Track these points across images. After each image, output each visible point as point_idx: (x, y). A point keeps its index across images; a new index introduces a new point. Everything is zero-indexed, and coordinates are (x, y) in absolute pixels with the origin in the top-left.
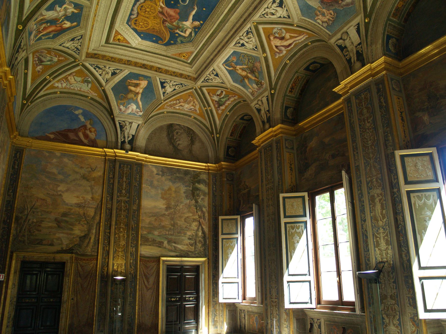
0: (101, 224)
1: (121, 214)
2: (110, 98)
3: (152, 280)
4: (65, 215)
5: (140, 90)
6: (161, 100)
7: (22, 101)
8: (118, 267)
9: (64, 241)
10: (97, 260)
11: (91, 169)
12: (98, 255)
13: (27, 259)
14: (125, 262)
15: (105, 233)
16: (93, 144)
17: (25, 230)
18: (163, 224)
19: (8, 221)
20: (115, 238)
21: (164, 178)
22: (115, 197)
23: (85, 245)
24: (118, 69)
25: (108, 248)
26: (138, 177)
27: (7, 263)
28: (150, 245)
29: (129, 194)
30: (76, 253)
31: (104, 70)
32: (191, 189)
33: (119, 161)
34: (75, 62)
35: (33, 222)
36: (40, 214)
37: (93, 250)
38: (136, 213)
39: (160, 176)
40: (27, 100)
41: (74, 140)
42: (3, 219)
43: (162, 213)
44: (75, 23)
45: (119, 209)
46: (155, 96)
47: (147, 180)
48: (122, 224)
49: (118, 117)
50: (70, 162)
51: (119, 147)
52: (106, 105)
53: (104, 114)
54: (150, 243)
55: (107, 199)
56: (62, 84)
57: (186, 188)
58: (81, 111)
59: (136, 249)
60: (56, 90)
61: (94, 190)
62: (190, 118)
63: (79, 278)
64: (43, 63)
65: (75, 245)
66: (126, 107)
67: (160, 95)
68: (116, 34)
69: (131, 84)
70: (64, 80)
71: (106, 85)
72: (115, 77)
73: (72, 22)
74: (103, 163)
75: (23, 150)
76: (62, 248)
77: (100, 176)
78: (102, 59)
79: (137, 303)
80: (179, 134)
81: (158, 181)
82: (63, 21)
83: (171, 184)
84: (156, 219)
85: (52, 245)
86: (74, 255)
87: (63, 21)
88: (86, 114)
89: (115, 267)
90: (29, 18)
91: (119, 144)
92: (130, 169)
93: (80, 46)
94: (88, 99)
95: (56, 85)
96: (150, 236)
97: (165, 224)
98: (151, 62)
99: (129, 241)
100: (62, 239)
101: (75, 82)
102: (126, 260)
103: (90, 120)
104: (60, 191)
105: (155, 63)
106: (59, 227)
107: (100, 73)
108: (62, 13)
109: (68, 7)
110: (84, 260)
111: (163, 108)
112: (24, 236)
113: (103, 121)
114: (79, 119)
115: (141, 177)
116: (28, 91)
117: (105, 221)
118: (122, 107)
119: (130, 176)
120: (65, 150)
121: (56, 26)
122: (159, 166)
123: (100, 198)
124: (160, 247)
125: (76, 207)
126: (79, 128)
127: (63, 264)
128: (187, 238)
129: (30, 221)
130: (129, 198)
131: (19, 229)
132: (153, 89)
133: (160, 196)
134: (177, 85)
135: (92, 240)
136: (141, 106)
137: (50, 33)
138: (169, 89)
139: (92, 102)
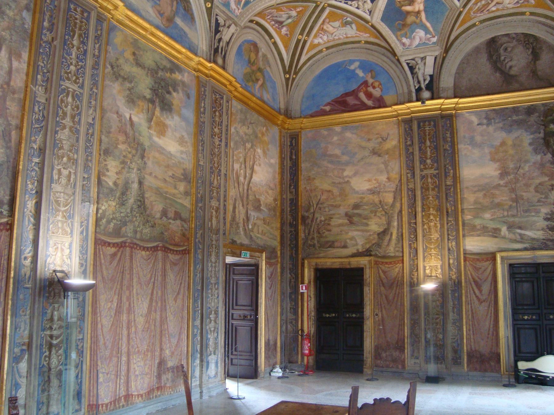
0: (403, 212)
1: (429, 195)
2: (384, 34)
3: (486, 288)
4: (356, 206)
6: (458, 9)
8: (431, 270)
9: (358, 241)
10: (403, 263)
11: (382, 138)
12: (403, 256)
13: (320, 267)
14: (441, 262)
15: (410, 223)
16: (380, 103)
17: (313, 231)
18: (497, 201)
19: (294, 223)
20: (423, 230)
21: (491, 129)
22: (418, 172)
23: (386, 244)
25: (415, 246)
26: (448, 135)
27: (300, 271)
28: (479, 236)
29: (438, 163)
30: (376, 256)
32: (542, 135)
34: (317, 6)
35: (321, 221)
36: (327, 210)
37: (397, 249)
38: (452, 190)
39: (485, 127)
40: (290, 74)
41: (355, 105)
42: (288, 222)
43: (495, 184)
45: (425, 188)
46: (445, 6)
47: (464, 137)
48: (431, 209)
50: (354, 136)
51: (414, 98)
52: (383, 44)
53: (388, 58)
54: (478, 233)
55: (407, 177)
56: (321, 37)
57: (532, 136)
58: (357, 64)
59: (456, 243)
60: (320, 48)
61: (389, 167)
62: (524, 17)
63: (382, 288)
64: (284, 24)
65: (373, 245)
66: (410, 38)
70: (320, 32)
74: (396, 126)
75: (298, 135)
76: (358, 250)
77: (395, 147)
79: (464, 321)
80: (509, 49)
81: (482, 135)
83: (504, 134)
84: (485, 194)
85: (345, 247)
86: (372, 257)
88: (364, 66)
89: (428, 272)
91: (414, 95)
92: (435, 126)
94: (362, 45)
95: (316, 41)
96: (477, 222)
97: (502, 200)
99: (444, 233)
100: (357, 238)
101: (335, 30)
102: (442, 260)
103: (371, 71)
104: (346, 177)
106: (351, 223)
107: (356, 6)
110: (386, 263)
111: (468, 17)
112: (313, 238)
113: (386, 67)
114: (357, 75)
115: (452, 134)
116: (287, 63)
117: (409, 207)
119: (436, 137)
120: (346, 121)
122: (481, 111)
123: (397, 176)
124: (496, 237)
125: (369, 194)
126: (359, 87)
127: (360, 271)
128: (541, 218)
129: (318, 220)
130: (437, 169)
131: (307, 232)
133: (489, 157)
135: (394, 237)
136: (431, 29)
139: (368, 46)
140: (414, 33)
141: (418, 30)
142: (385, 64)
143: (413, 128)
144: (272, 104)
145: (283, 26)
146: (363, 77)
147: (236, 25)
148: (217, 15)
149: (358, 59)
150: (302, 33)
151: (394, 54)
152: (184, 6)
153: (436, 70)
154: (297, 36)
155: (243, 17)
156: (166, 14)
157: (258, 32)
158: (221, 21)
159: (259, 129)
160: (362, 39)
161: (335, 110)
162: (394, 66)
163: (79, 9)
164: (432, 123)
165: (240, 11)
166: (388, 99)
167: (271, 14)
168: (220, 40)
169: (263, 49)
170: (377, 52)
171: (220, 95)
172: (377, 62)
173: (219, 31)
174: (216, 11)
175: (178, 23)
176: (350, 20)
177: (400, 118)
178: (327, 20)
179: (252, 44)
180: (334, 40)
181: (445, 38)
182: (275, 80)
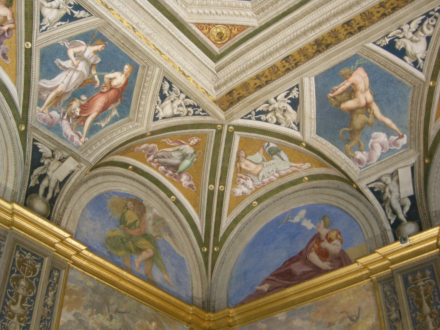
2: (327, 154)
5: (365, 96)
6: (424, 82)
7: (201, 251)
24: (291, 90)
31: (274, 110)
33: (401, 271)
34: (219, 133)
40: (206, 244)
41: (304, 273)
46: (404, 84)
49: (363, 179)
50: (306, 322)
52: (333, 172)
53: (344, 191)
56: (243, 184)
58: (303, 213)
60: (247, 202)
66: (367, 149)
67: (412, 74)
68: (206, 31)
69: (339, 98)
70: (240, 175)
71: (303, 135)
72: (303, 106)
73: (121, 70)
74: (370, 293)
78: (250, 93)
82: (101, 78)
87: (101, 78)
88: (313, 213)
90: (26, 107)
91: (390, 234)
93: (187, 97)
95: (239, 191)
98: (320, 24)
101: (260, 168)
103: (323, 218)
105: (327, 20)
107: (275, 120)
108: (82, 66)
109: (77, 50)
113: (343, 205)
114: (305, 228)
116: (201, 230)
118: (359, 155)
121: (102, 93)
132: (386, 73)
134: (421, 25)
136: (394, 126)
137: (105, 108)
138: (418, 49)
139: (315, 183)
140: (371, 141)
141: (375, 134)
142: (341, 202)
143: (397, 290)
144: (174, 289)
145: (180, 173)
146: (313, 228)
147: (77, 158)
148: (34, 140)
149: (302, 205)
150: (212, 181)
151: (350, 182)
153: (417, 186)
154: (206, 187)
155: (90, 148)
157: (144, 185)
159: (139, 322)
160: (304, 174)
161: (277, 288)
162: (354, 201)
164: (428, 272)
165: (83, 140)
166: (350, 252)
167: (151, 151)
168: (42, 177)
169: (155, 207)
170: (328, 188)
172: (328, 202)
173: (43, 164)
174: (32, 135)
176: (275, 145)
177: (374, 277)
178: (243, 154)
179: (131, 200)
180: (264, 185)
181: (419, 135)
182: (182, 255)
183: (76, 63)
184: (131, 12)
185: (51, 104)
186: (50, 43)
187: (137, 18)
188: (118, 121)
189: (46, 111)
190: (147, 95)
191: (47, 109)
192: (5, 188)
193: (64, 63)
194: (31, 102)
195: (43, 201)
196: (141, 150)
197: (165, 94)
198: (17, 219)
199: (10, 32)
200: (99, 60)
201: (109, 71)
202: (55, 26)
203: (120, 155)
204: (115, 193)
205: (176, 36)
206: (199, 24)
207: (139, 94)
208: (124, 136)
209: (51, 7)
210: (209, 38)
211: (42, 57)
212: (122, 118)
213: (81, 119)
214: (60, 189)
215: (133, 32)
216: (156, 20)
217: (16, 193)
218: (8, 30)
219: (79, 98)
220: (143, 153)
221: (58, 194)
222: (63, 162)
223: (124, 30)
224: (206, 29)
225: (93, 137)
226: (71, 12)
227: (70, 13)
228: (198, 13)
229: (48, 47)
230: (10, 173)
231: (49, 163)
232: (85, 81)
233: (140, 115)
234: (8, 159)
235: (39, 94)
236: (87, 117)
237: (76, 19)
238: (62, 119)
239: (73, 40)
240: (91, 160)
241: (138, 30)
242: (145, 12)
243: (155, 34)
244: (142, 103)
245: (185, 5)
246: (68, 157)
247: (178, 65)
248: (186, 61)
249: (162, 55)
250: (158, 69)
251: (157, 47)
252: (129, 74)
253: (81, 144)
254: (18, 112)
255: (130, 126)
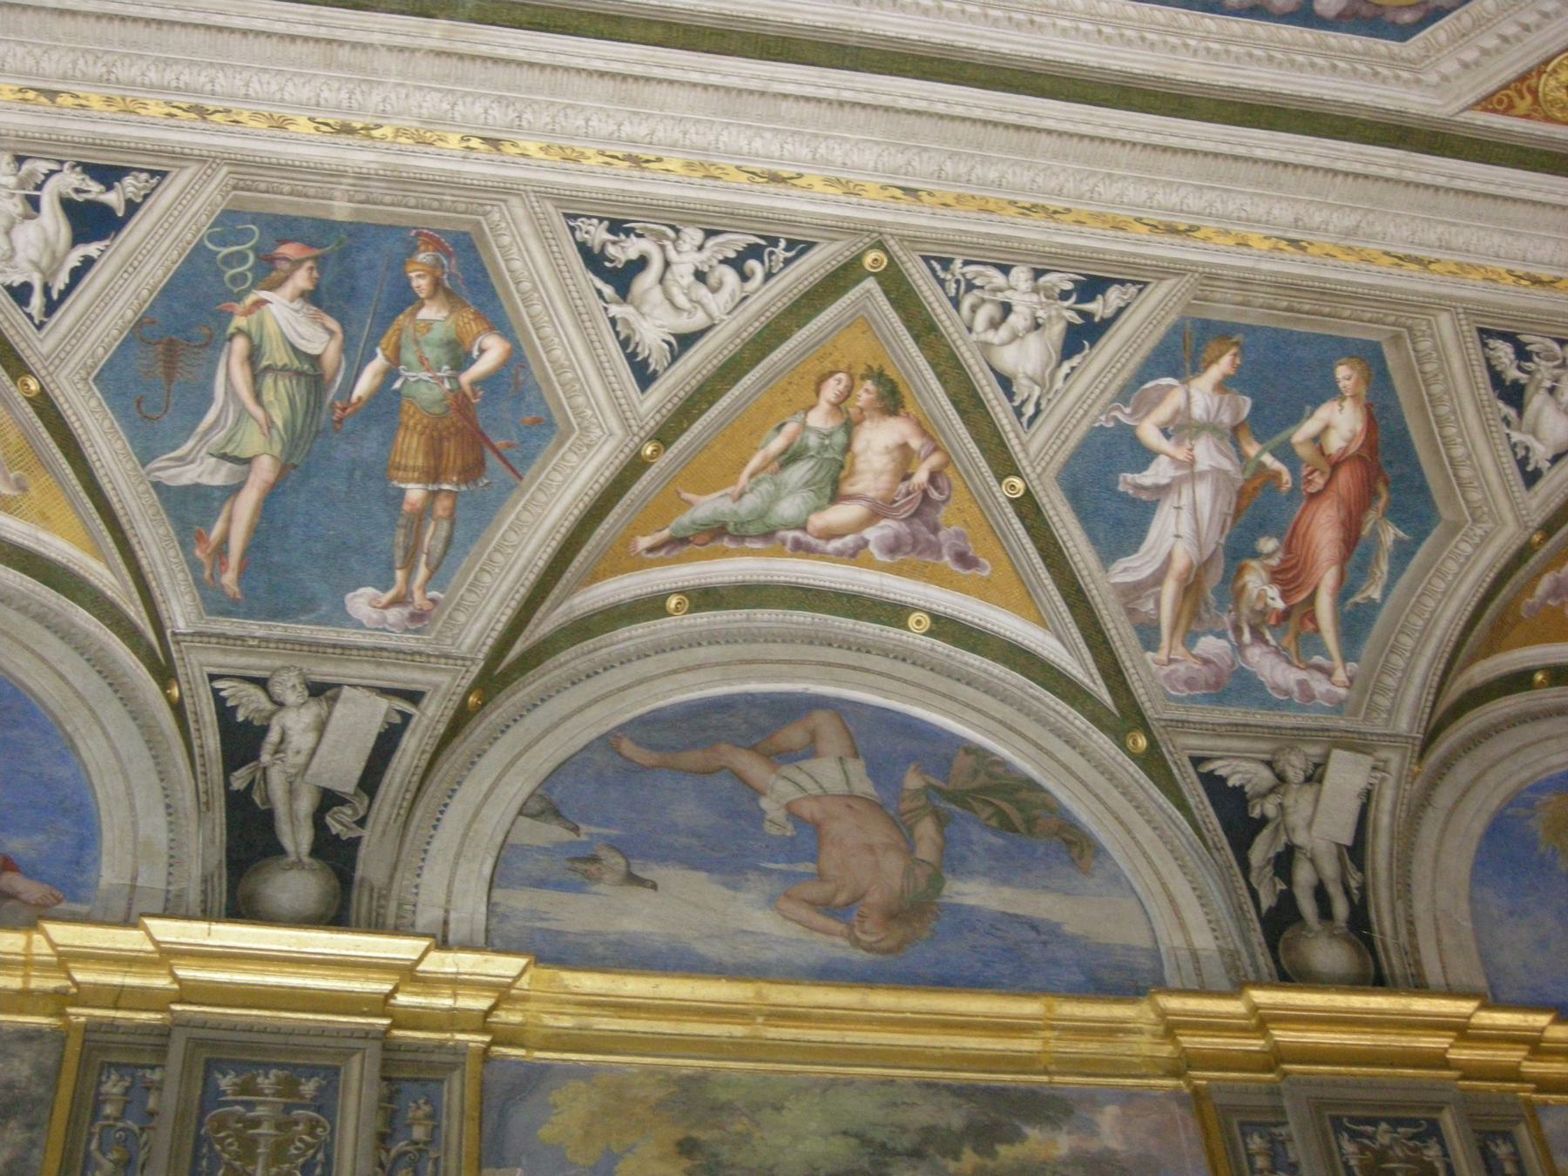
44: (1342, 372)
68: (1524, 105)
73: (1331, 391)
82: (1286, 453)
87: (1286, 453)
90: (1113, 672)
108: (1206, 453)
109: (1163, 412)
121: (1313, 497)
137: (1351, 537)
147: (1357, 744)
148: (1197, 761)
152: (1000, 813)
155: (1379, 689)
156: (874, 897)
158: (1243, 772)
163: (266, 1082)
165: (1340, 675)
168: (1284, 863)
171: (1396, 1123)
173: (1263, 821)
174: (1179, 749)
175: (970, 901)
183: (1181, 454)
184: (1256, 200)
185: (1183, 622)
186: (1072, 443)
187: (1284, 204)
188: (1413, 554)
189: (1180, 652)
190: (1457, 420)
191: (1177, 642)
192: (1194, 955)
193: (1148, 478)
194: (1122, 651)
195: (1332, 936)
196: (1543, 604)
197: (1515, 382)
198: (1284, 1036)
199: (941, 482)
200: (1246, 404)
201: (1296, 418)
202: (1059, 384)
203: (1486, 656)
204: (1537, 788)
205: (1441, 181)
206: (1488, 98)
207: (1431, 432)
208: (1464, 589)
209: (1015, 337)
210: (1548, 119)
211: (1075, 495)
212: (1418, 541)
213: (1299, 615)
214: (1361, 868)
215: (1299, 256)
216: (1347, 174)
217: (1234, 955)
218: (933, 478)
219: (1256, 555)
220: (1553, 610)
221: (1363, 888)
222: (1320, 781)
223: (1265, 266)
224: (1522, 97)
225: (1367, 649)
226: (1081, 313)
227: (1078, 321)
228: (1466, 66)
229: (1077, 455)
230: (1180, 900)
231: (1281, 807)
232: (1241, 493)
233: (1475, 496)
234: (1150, 863)
235: (1131, 612)
236: (1312, 599)
237: (1107, 323)
238: (1240, 648)
239: (1132, 391)
240: (1403, 724)
241: (1310, 238)
242: (1300, 171)
243: (1371, 217)
244: (1458, 452)
245: (1410, 70)
246: (1327, 756)
247: (1501, 267)
248: (1520, 235)
249: (1432, 267)
250: (1444, 320)
251: (1401, 251)
252: (1363, 390)
253: (1342, 692)
254: (1098, 703)
255: (1464, 546)
